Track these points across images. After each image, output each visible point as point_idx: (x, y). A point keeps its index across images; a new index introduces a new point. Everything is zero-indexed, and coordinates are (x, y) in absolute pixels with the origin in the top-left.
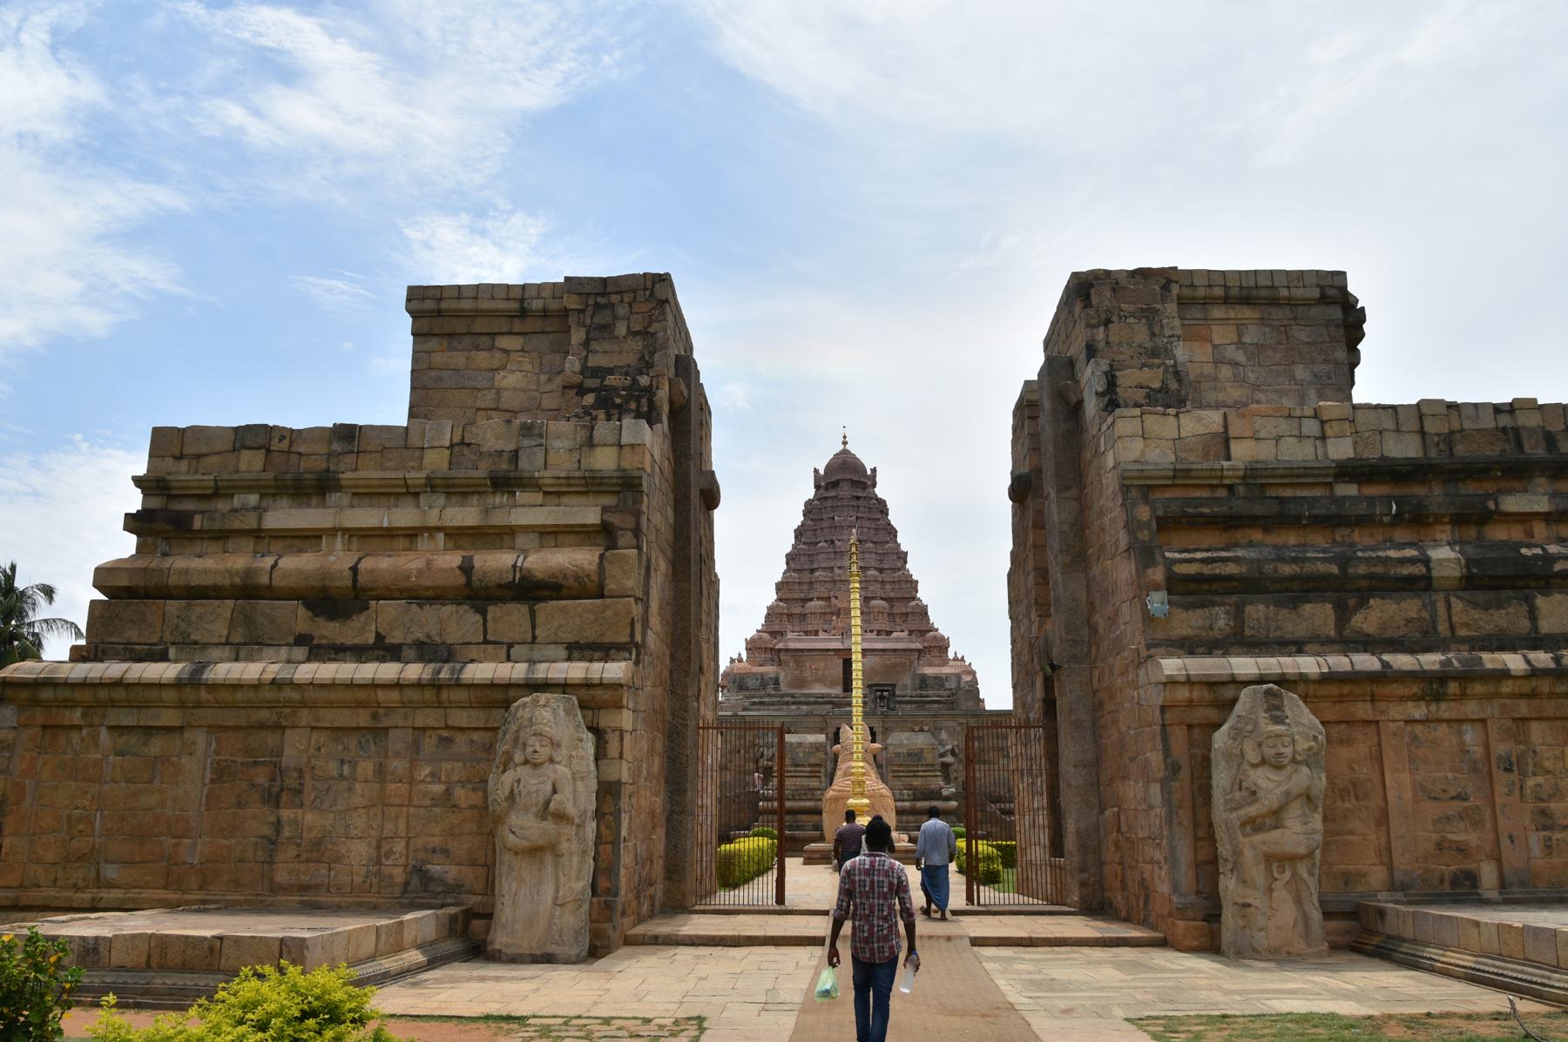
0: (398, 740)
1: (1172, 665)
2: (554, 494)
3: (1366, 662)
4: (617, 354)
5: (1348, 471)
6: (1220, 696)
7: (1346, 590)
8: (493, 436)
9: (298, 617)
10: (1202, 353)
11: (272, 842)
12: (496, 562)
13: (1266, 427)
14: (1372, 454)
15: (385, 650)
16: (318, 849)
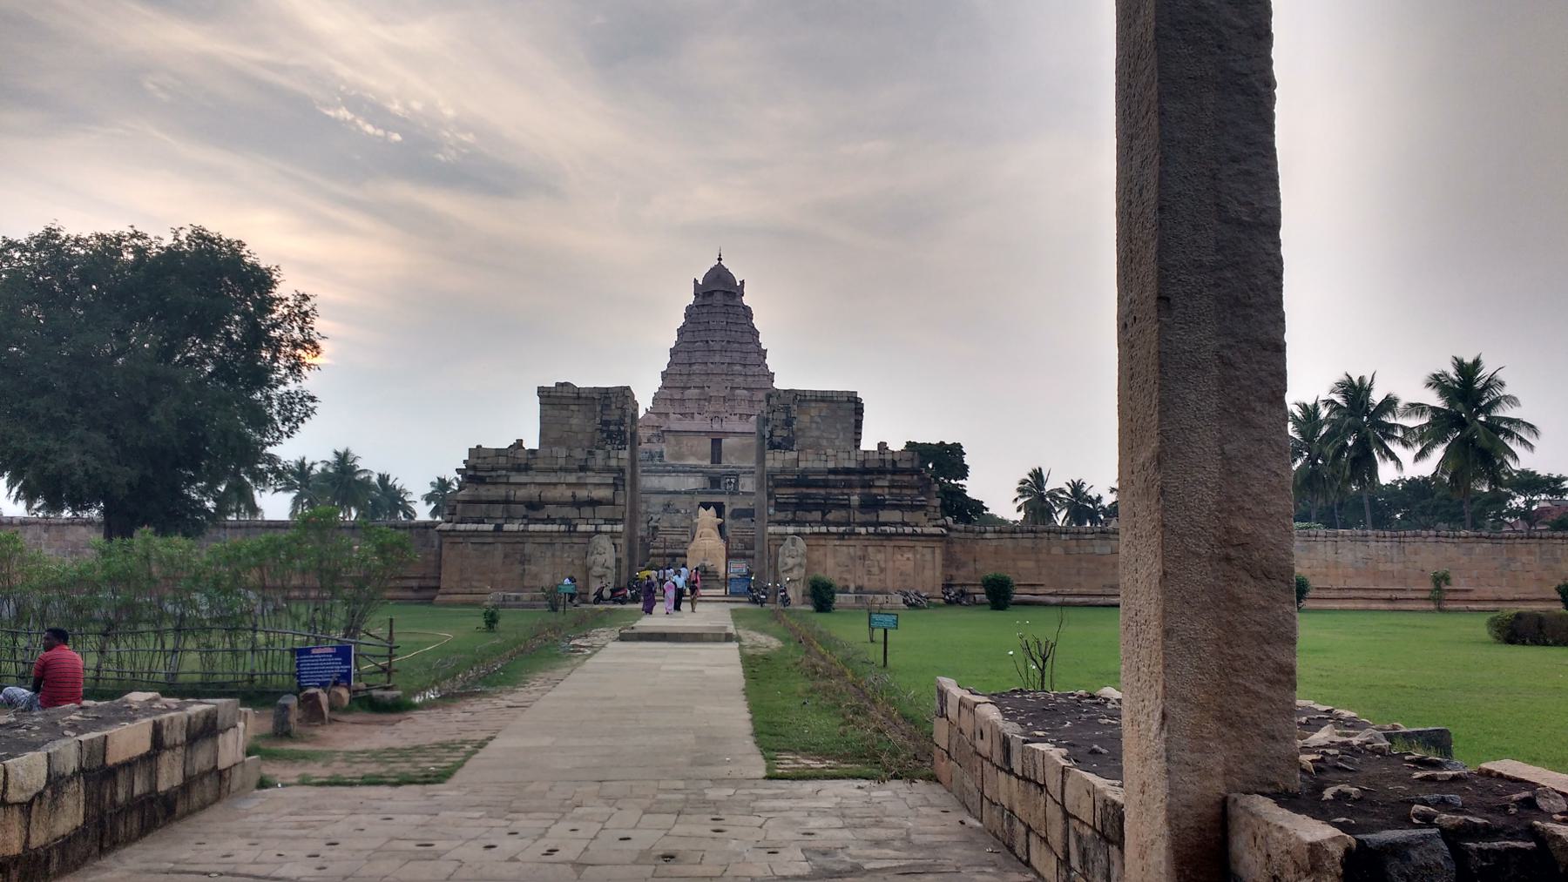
0: (557, 546)
1: (771, 529)
2: (600, 471)
3: (824, 529)
4: (615, 415)
5: (831, 471)
6: (783, 536)
7: (825, 507)
8: (579, 454)
9: (521, 509)
10: (806, 419)
11: (522, 575)
12: (582, 494)
13: (810, 457)
14: (840, 466)
15: (553, 521)
16: (535, 576)
